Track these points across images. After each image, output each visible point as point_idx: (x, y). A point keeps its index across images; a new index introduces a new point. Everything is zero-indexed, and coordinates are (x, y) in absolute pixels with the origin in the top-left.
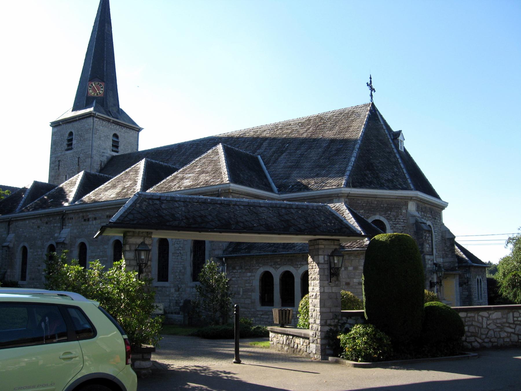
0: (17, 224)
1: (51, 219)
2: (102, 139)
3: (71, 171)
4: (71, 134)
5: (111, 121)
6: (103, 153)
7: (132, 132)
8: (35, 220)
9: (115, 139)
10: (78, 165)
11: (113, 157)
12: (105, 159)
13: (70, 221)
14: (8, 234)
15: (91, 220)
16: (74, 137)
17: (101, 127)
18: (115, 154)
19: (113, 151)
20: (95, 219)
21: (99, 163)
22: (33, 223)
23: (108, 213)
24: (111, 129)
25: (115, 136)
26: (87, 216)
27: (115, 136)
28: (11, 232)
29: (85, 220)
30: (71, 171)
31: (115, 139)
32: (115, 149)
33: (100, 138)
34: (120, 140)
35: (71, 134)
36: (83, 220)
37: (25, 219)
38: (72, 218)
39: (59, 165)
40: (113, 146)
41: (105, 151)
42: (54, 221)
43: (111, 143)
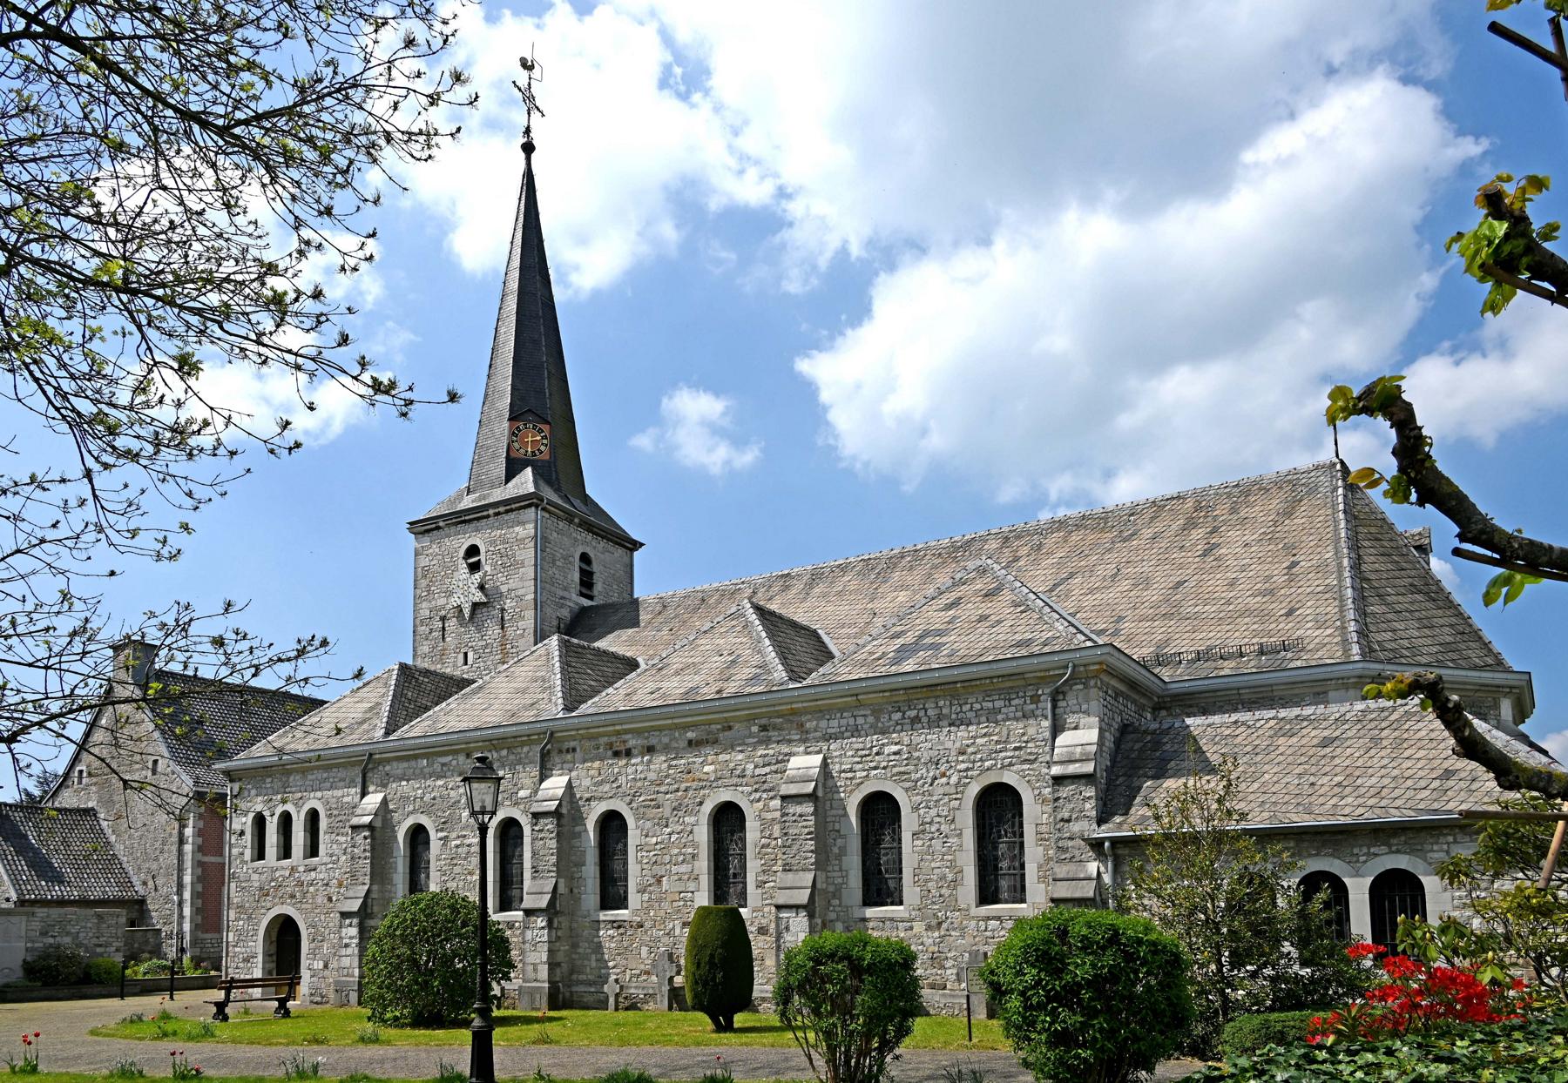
0: (388, 768)
1: (504, 752)
2: (558, 563)
3: (480, 643)
4: (473, 551)
5: (576, 520)
6: (562, 598)
7: (620, 552)
8: (450, 758)
9: (584, 566)
10: (502, 628)
11: (584, 609)
12: (565, 613)
13: (569, 757)
14: (364, 794)
15: (635, 752)
16: (482, 557)
17: (555, 535)
18: (586, 602)
19: (582, 595)
20: (650, 750)
21: (555, 623)
22: (443, 765)
23: (690, 735)
24: (576, 540)
25: (585, 558)
26: (624, 742)
27: (585, 558)
28: (371, 788)
29: (617, 754)
30: (480, 643)
31: (584, 566)
32: (584, 591)
33: (554, 561)
34: (596, 567)
35: (473, 551)
36: (610, 753)
37: (416, 757)
38: (574, 750)
39: (444, 628)
40: (582, 583)
41: (566, 594)
42: (512, 757)
43: (577, 576)
